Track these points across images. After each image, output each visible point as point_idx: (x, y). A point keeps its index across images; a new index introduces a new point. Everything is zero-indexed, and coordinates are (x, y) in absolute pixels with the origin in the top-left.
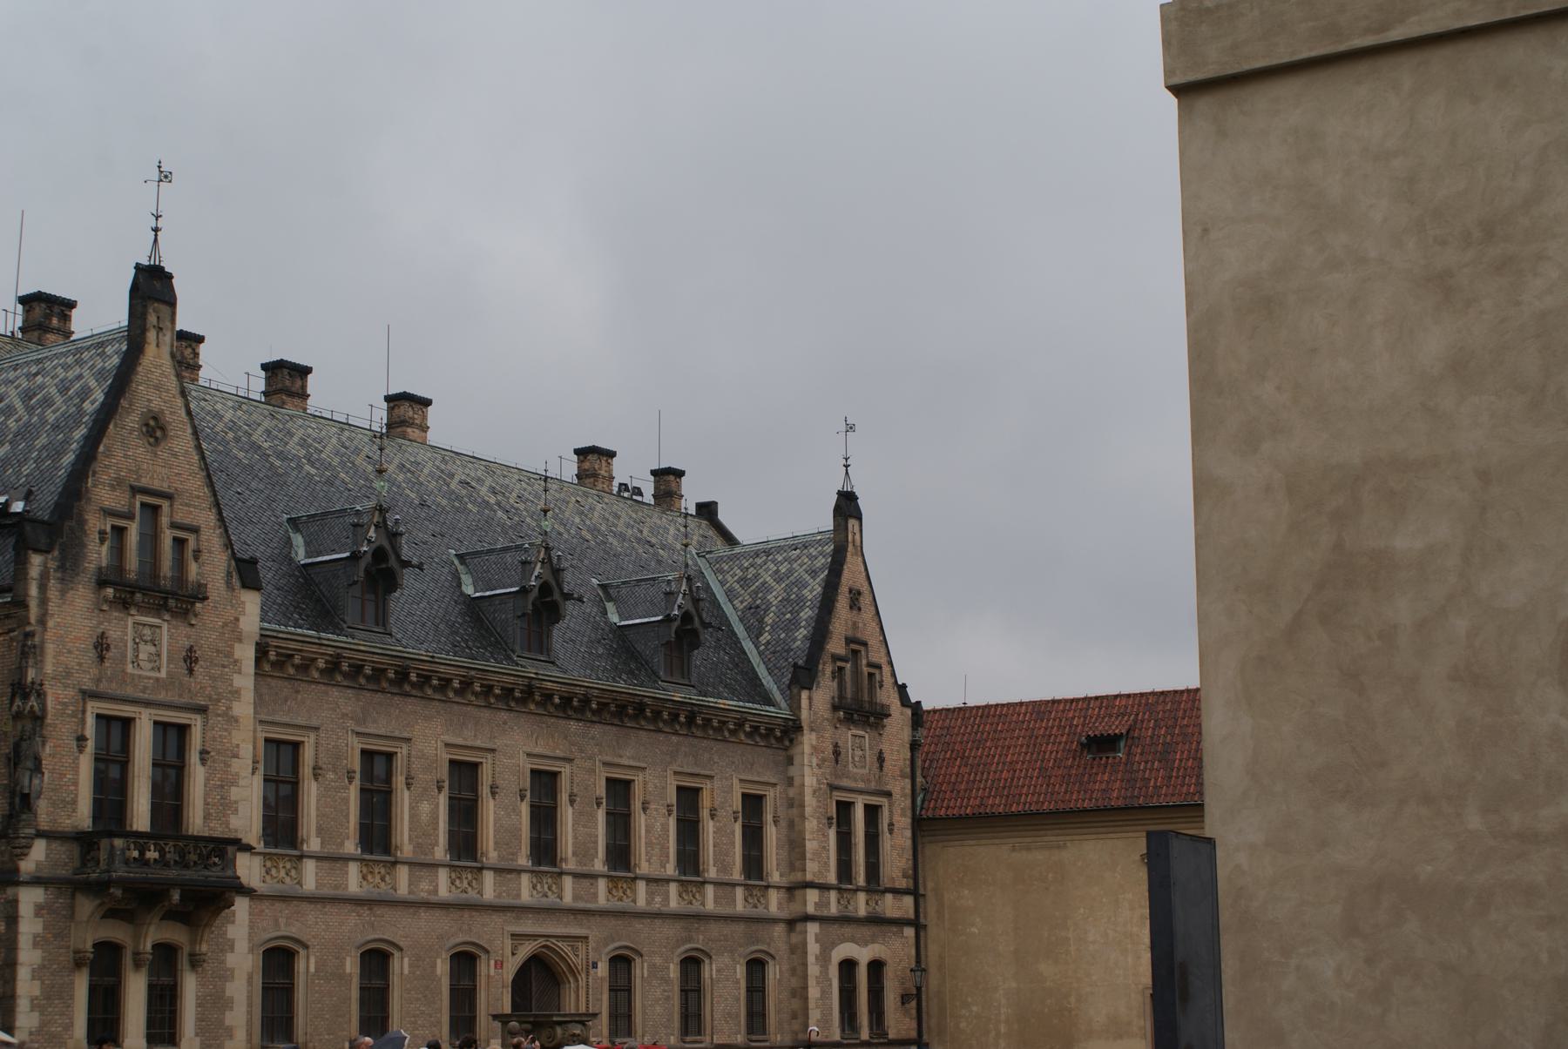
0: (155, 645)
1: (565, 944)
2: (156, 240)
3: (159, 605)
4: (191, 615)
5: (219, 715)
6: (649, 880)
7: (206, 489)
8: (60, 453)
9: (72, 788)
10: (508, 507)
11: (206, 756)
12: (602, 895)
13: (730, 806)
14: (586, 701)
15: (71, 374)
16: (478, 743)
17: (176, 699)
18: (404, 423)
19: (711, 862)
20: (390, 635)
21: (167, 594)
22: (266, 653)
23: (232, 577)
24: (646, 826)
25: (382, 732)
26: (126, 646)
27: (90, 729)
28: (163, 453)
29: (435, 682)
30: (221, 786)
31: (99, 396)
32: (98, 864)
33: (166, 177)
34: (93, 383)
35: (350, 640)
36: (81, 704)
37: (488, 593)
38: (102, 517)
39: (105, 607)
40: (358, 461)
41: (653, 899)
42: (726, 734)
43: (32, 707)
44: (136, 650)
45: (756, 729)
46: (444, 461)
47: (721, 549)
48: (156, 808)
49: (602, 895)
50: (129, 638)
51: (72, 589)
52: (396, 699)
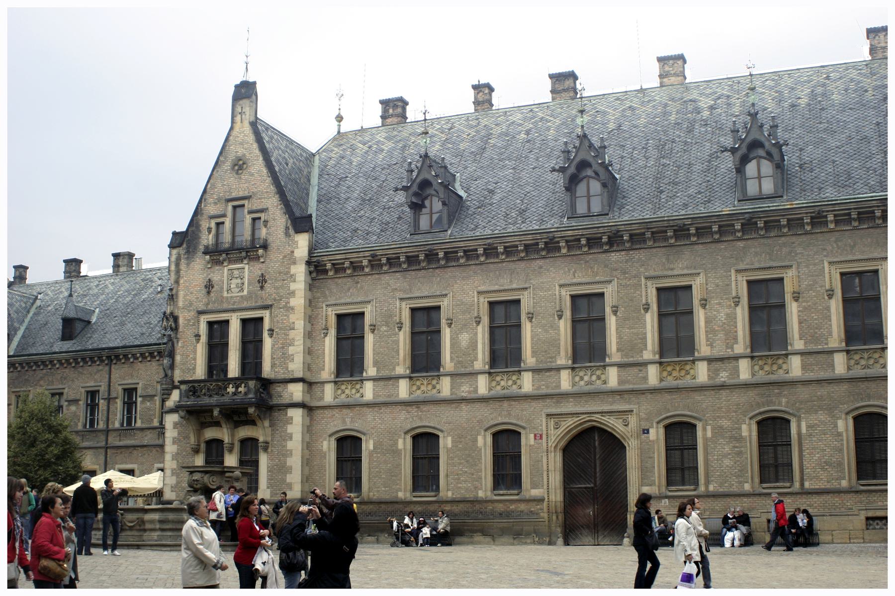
0: (242, 279)
1: (611, 418)
2: (247, 68)
5: (281, 308)
7: (271, 187)
13: (821, 287)
16: (514, 286)
17: (253, 304)
24: (706, 318)
25: (426, 294)
28: (245, 176)
51: (193, 261)
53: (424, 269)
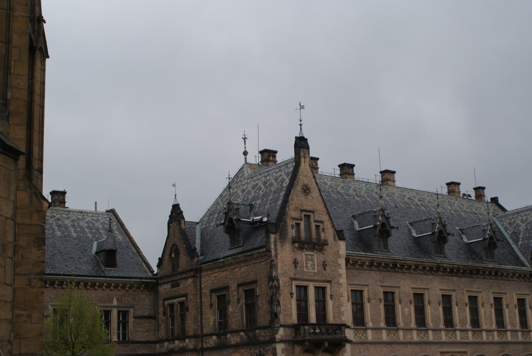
0: (312, 261)
1: (459, 354)
2: (301, 128)
3: (313, 248)
4: (323, 250)
5: (335, 283)
6: (487, 331)
8: (277, 201)
9: (290, 310)
10: (425, 205)
11: (332, 297)
12: (470, 337)
13: (513, 303)
14: (458, 270)
15: (278, 175)
16: (423, 287)
17: (321, 279)
18: (387, 180)
19: (508, 323)
20: (389, 252)
21: (315, 244)
22: (349, 261)
23: (335, 237)
24: (484, 312)
25: (390, 285)
26: (303, 262)
27: (294, 290)
28: (309, 198)
29: (406, 267)
30: (338, 306)
31: (287, 181)
32: (301, 334)
33: (302, 107)
34: (285, 177)
35: (376, 255)
36: (291, 283)
37: (421, 235)
38: (292, 220)
39: (295, 250)
40: (373, 194)
41: (489, 337)
42: (509, 278)
43: (275, 284)
44: (307, 263)
45: (520, 275)
46: (402, 191)
47: (501, 213)
48: (317, 315)
49: (470, 337)
50: (304, 259)
51: (285, 245)
52: (393, 273)
53: (389, 271)
